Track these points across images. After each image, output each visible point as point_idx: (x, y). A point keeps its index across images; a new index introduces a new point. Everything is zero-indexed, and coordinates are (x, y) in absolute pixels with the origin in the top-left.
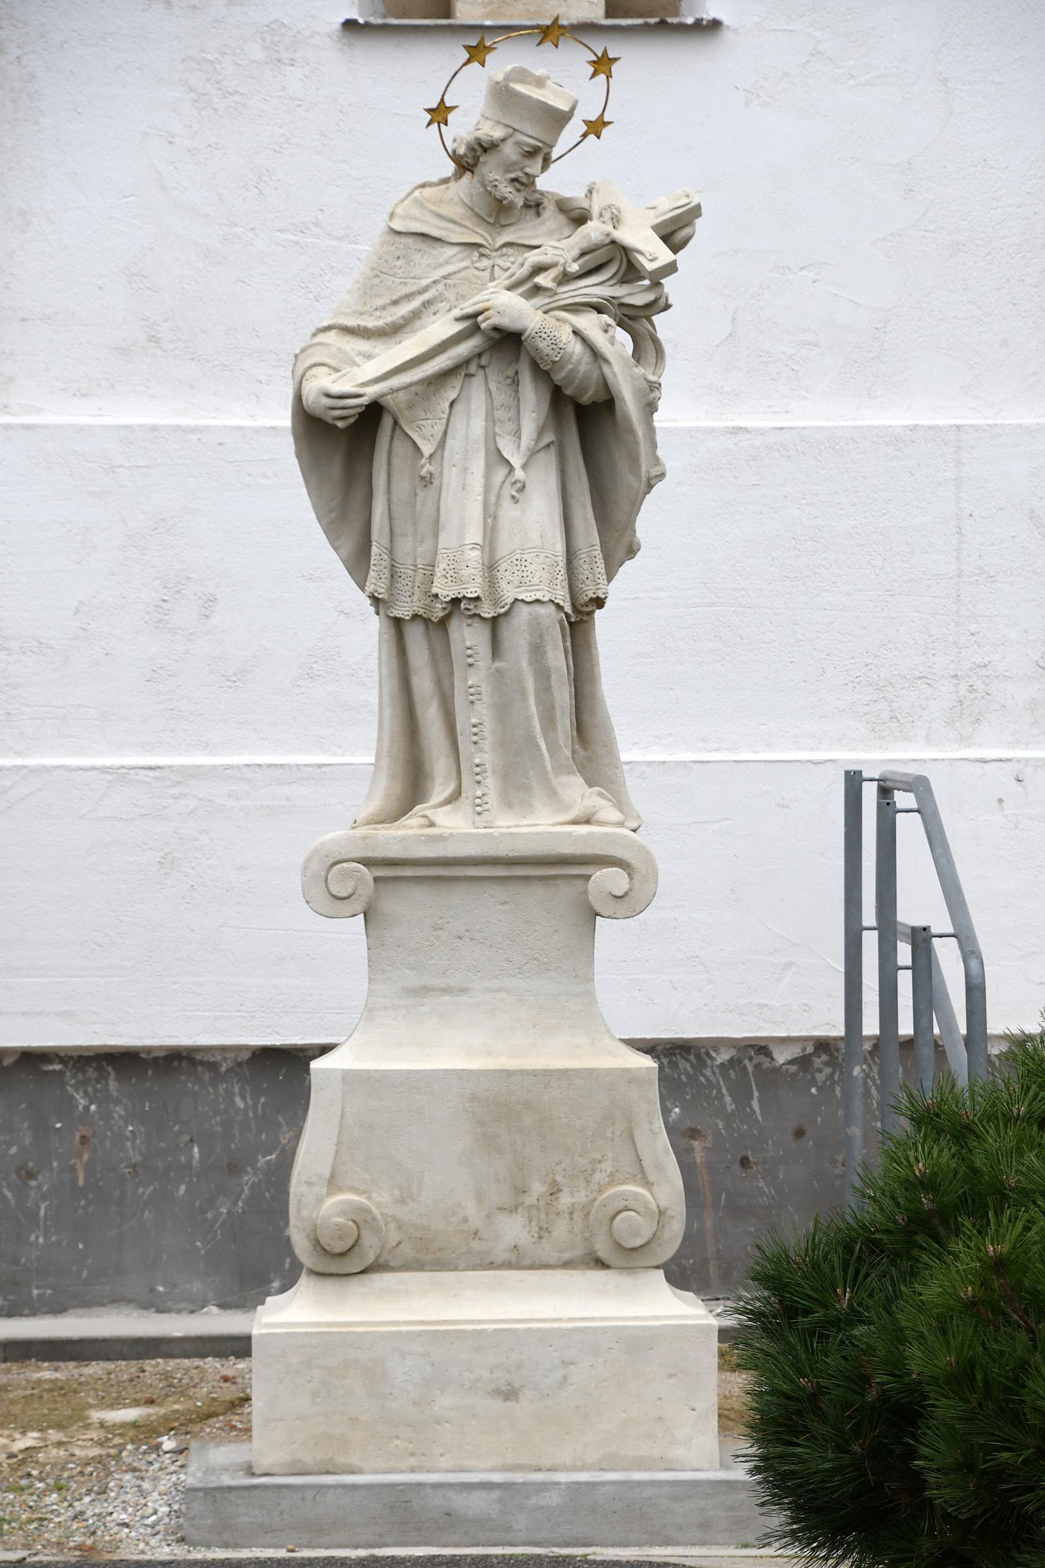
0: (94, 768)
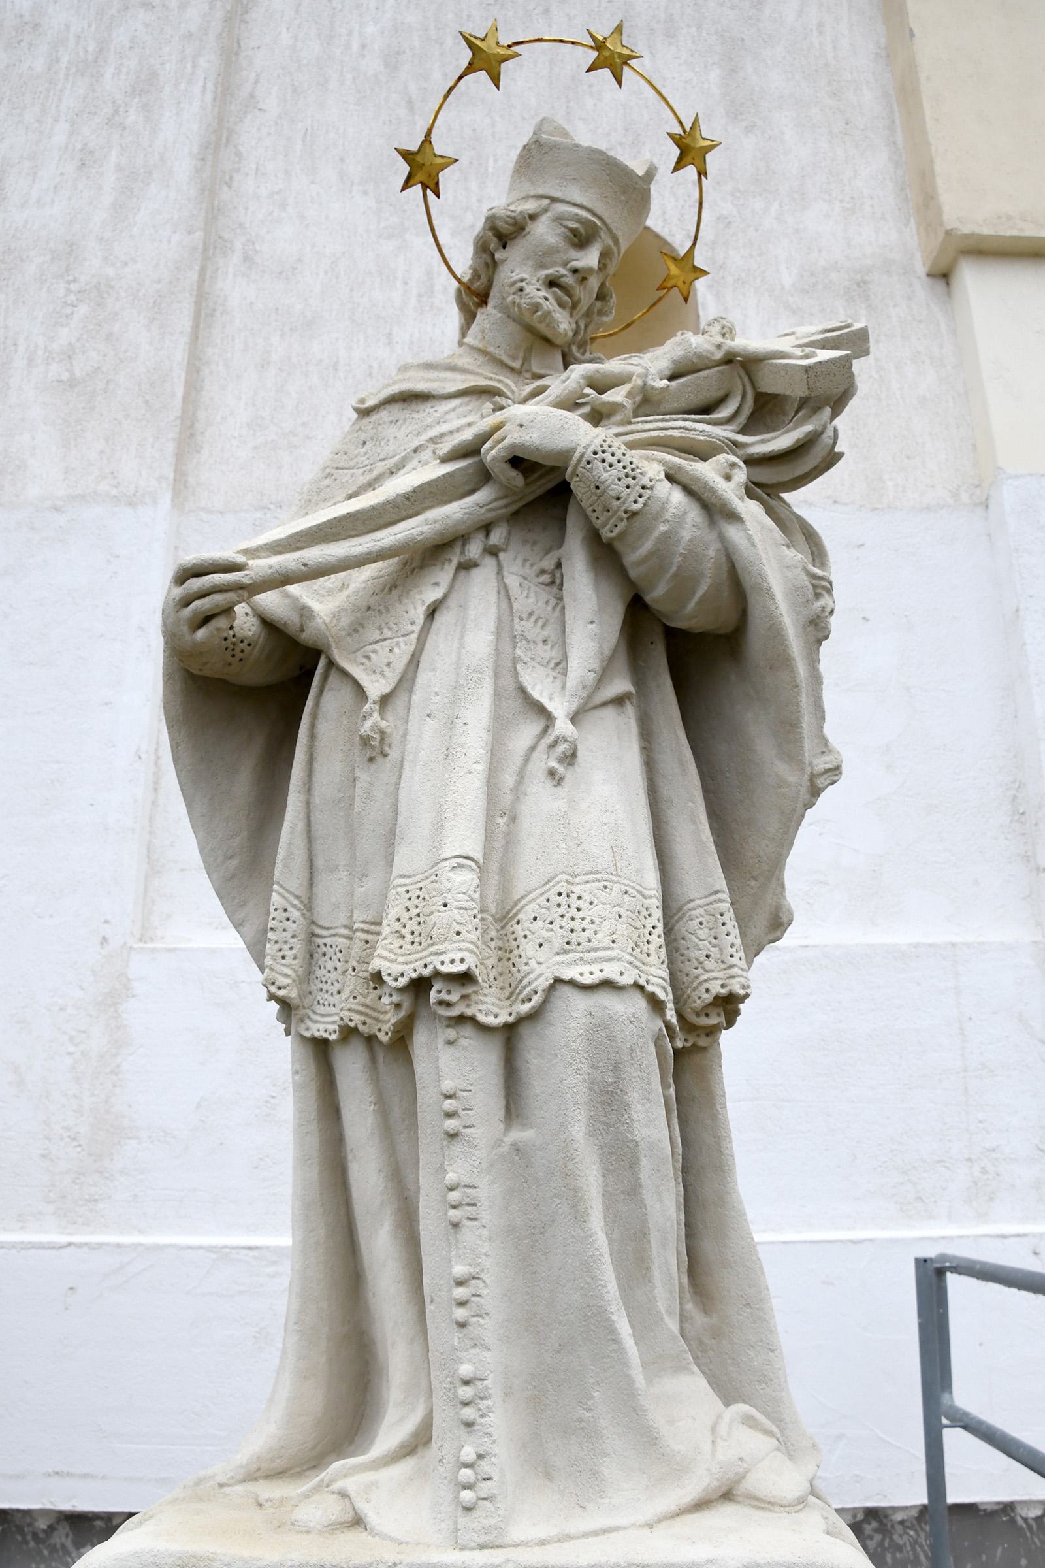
0: (200, 1247)
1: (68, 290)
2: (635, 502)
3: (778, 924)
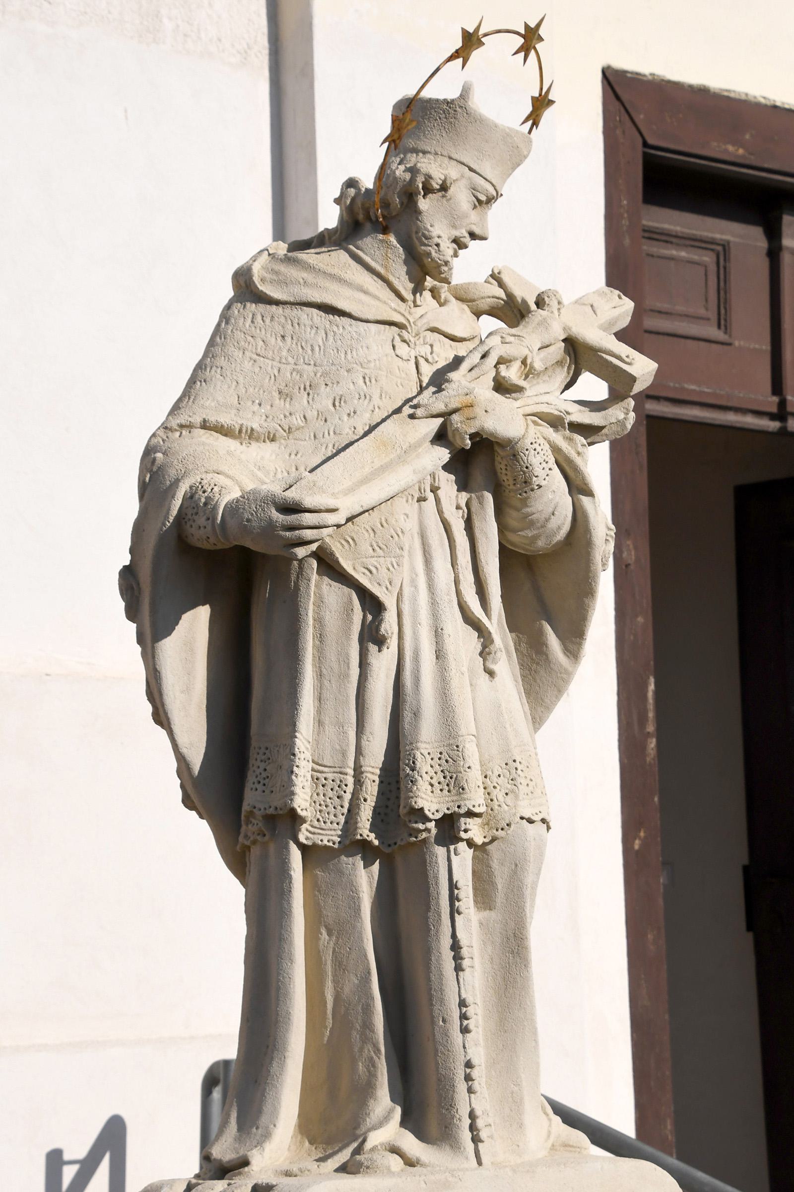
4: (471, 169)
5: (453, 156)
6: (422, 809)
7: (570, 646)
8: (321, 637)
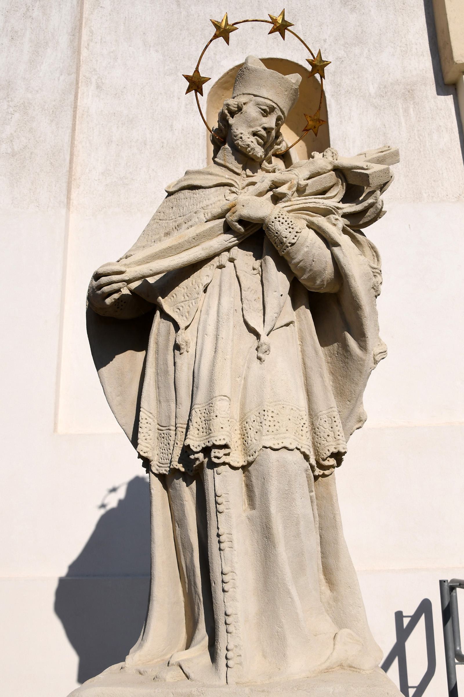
1: (9, 106)
2: (294, 239)
3: (361, 420)
4: (255, 96)
5: (245, 92)
6: (189, 445)
7: (362, 344)
8: (157, 352)
